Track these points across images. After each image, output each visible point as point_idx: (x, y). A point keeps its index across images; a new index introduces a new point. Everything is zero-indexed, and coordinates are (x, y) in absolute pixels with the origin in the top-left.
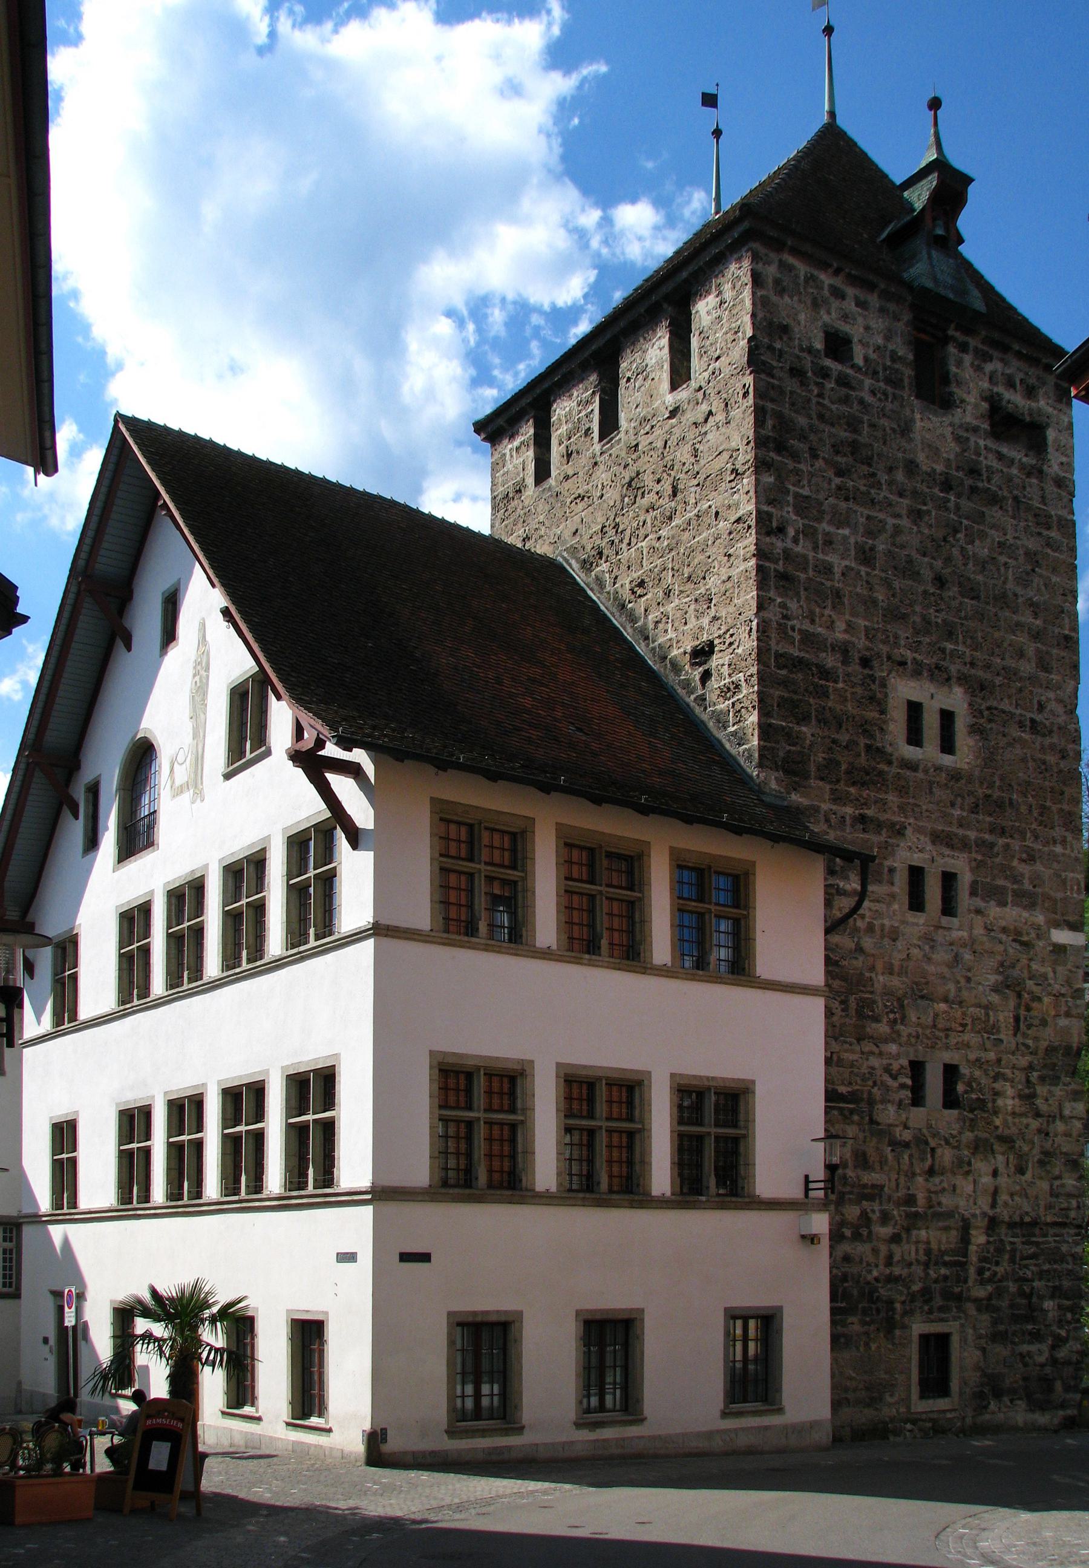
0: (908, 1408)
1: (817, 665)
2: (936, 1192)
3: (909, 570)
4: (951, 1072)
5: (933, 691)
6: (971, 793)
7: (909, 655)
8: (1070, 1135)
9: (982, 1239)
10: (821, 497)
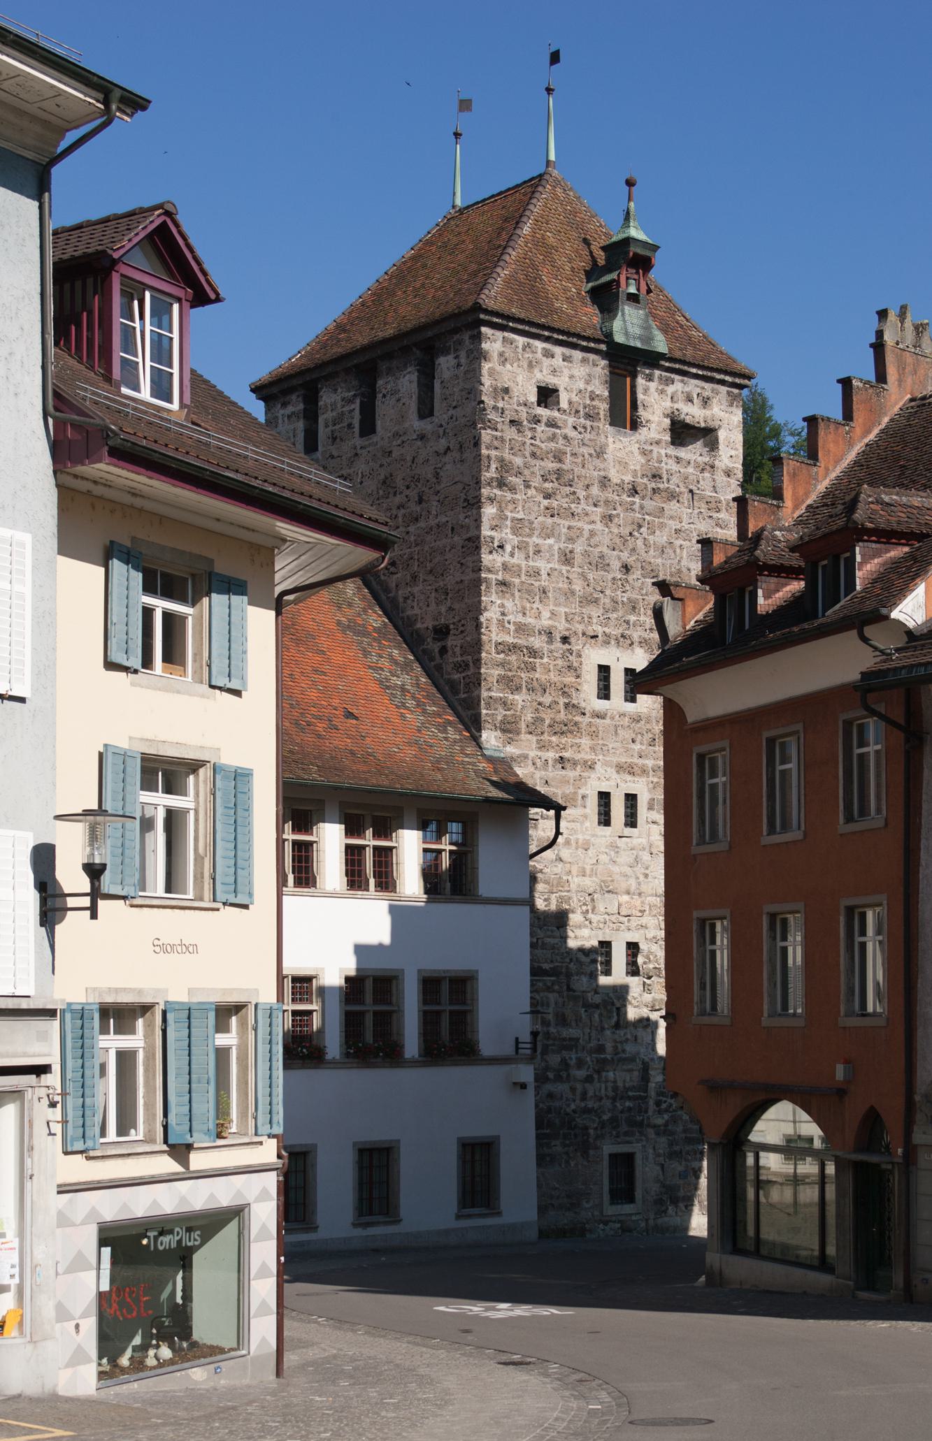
0: (602, 1212)
1: (527, 648)
3: (601, 564)
5: (619, 654)
6: (649, 731)
7: (600, 630)
10: (532, 518)
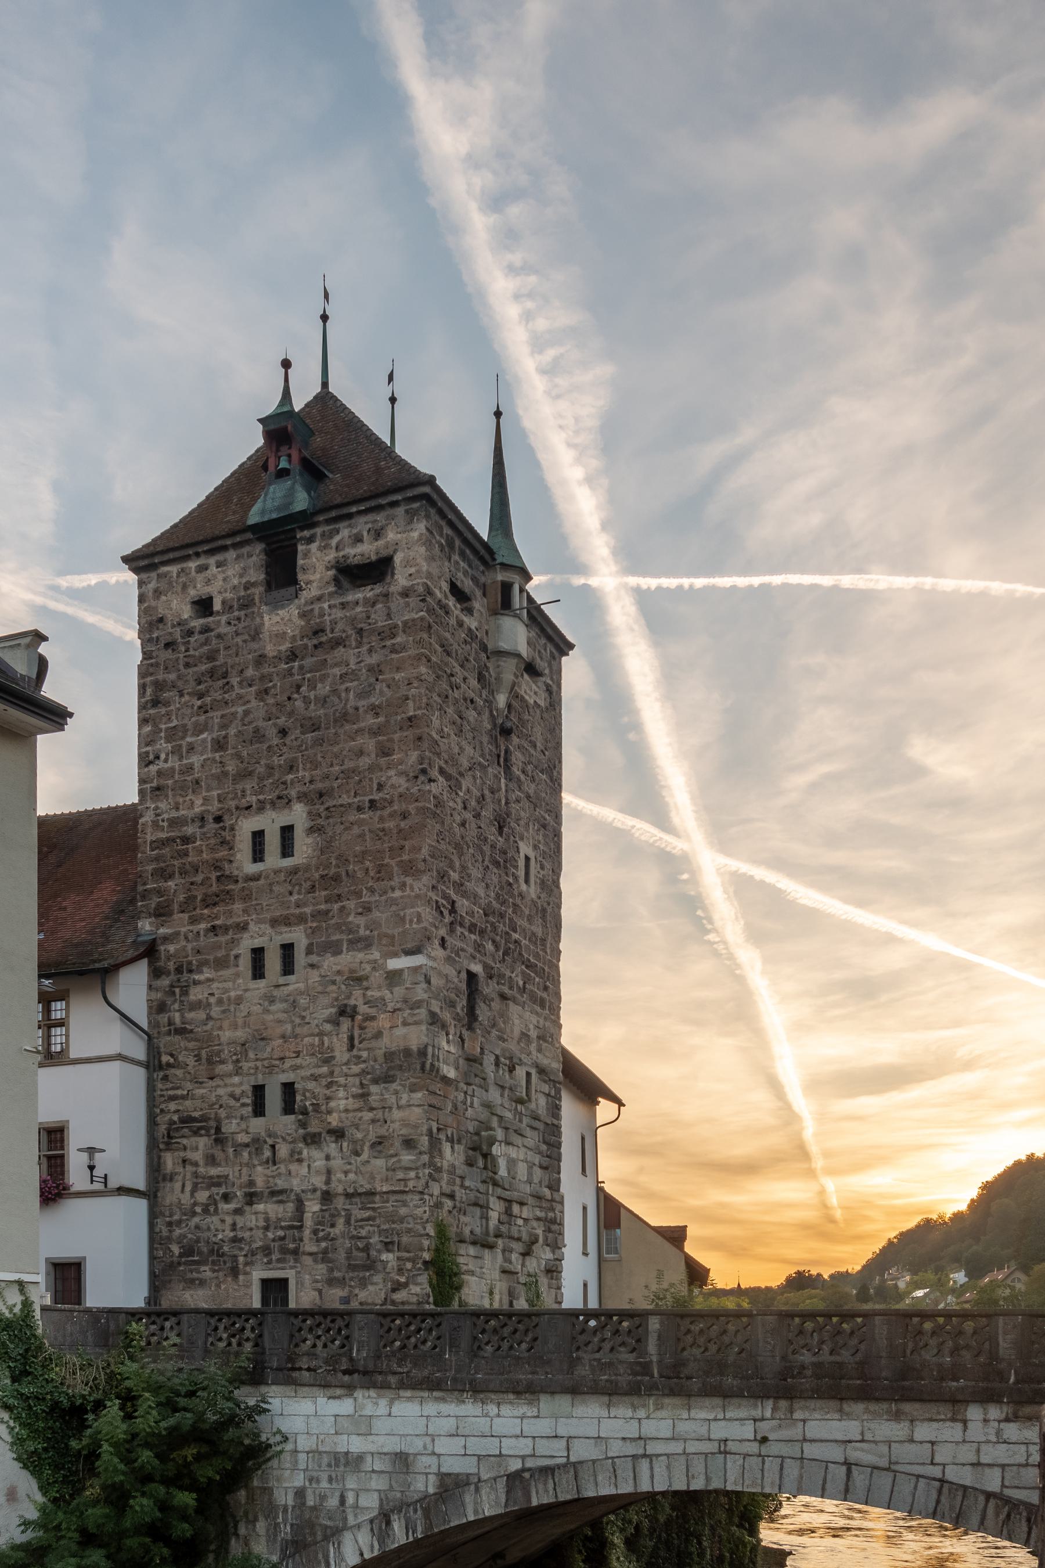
2: (273, 1177)
4: (289, 1088)
9: (316, 1208)
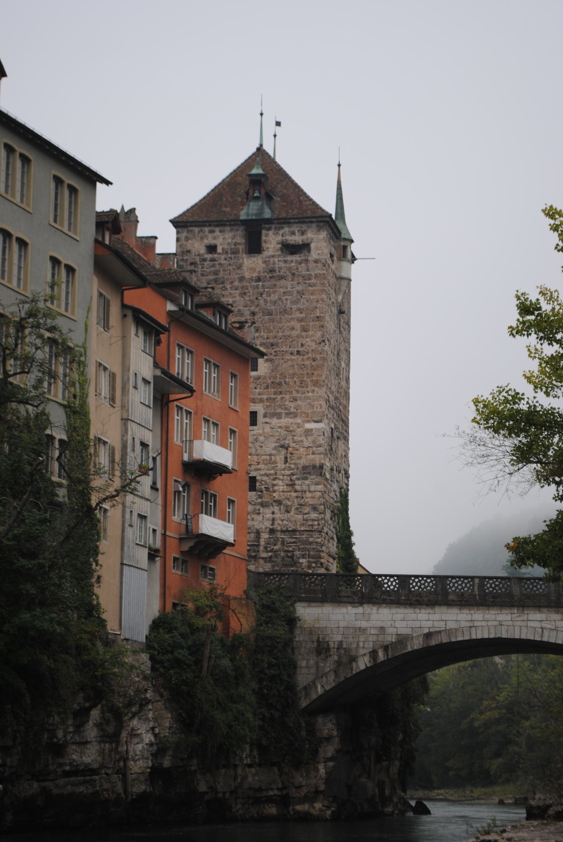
8: (314, 498)
